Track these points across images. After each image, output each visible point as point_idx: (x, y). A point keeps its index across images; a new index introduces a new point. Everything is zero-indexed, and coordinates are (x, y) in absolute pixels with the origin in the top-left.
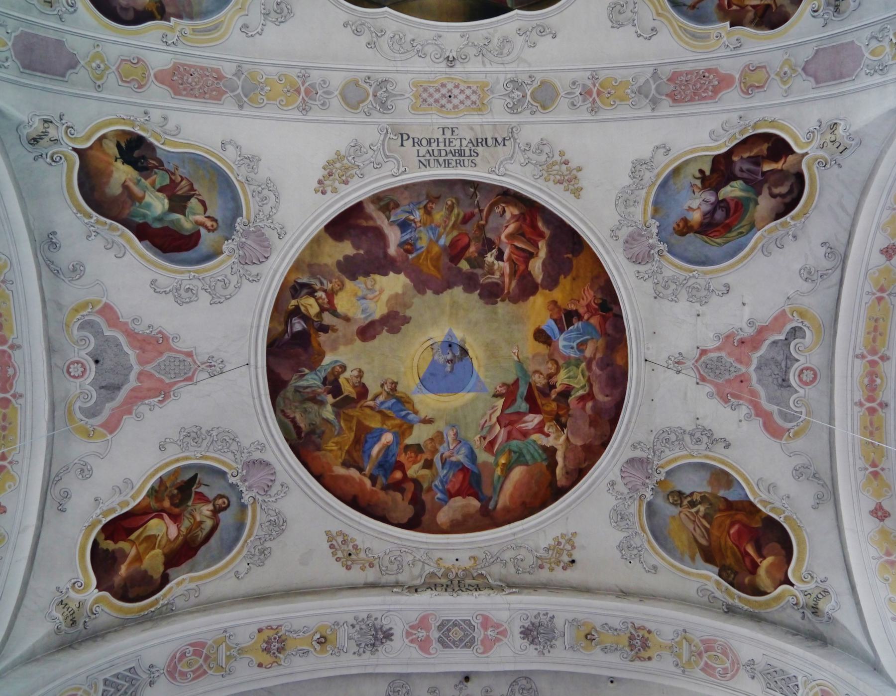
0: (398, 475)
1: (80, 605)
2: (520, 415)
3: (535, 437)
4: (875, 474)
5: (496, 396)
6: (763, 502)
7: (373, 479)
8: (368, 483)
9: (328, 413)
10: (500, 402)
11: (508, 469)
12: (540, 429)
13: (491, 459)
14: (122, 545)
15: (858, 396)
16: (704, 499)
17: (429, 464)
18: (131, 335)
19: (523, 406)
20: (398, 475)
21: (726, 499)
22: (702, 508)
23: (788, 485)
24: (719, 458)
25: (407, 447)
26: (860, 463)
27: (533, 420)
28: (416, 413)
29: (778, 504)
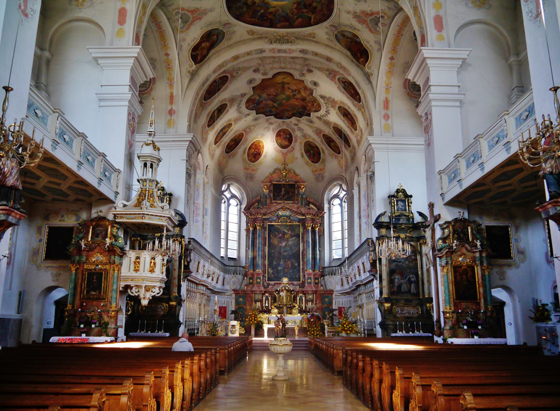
0: (266, 18)
1: (193, 71)
2: (302, 9)
3: (306, 14)
4: (394, 50)
5: (295, 3)
6: (365, 45)
7: (259, 19)
8: (257, 20)
9: (245, 9)
10: (296, 5)
11: (297, 19)
12: (307, 12)
13: (292, 16)
14: (197, 52)
15: (395, 33)
16: (350, 38)
17: (275, 16)
18: (188, 11)
19: (302, 6)
20: (266, 18)
21: (356, 40)
22: (349, 40)
23: (372, 43)
24: (355, 32)
25: (268, 13)
26: (391, 47)
27: (305, 10)
28: (270, 5)
29: (368, 46)
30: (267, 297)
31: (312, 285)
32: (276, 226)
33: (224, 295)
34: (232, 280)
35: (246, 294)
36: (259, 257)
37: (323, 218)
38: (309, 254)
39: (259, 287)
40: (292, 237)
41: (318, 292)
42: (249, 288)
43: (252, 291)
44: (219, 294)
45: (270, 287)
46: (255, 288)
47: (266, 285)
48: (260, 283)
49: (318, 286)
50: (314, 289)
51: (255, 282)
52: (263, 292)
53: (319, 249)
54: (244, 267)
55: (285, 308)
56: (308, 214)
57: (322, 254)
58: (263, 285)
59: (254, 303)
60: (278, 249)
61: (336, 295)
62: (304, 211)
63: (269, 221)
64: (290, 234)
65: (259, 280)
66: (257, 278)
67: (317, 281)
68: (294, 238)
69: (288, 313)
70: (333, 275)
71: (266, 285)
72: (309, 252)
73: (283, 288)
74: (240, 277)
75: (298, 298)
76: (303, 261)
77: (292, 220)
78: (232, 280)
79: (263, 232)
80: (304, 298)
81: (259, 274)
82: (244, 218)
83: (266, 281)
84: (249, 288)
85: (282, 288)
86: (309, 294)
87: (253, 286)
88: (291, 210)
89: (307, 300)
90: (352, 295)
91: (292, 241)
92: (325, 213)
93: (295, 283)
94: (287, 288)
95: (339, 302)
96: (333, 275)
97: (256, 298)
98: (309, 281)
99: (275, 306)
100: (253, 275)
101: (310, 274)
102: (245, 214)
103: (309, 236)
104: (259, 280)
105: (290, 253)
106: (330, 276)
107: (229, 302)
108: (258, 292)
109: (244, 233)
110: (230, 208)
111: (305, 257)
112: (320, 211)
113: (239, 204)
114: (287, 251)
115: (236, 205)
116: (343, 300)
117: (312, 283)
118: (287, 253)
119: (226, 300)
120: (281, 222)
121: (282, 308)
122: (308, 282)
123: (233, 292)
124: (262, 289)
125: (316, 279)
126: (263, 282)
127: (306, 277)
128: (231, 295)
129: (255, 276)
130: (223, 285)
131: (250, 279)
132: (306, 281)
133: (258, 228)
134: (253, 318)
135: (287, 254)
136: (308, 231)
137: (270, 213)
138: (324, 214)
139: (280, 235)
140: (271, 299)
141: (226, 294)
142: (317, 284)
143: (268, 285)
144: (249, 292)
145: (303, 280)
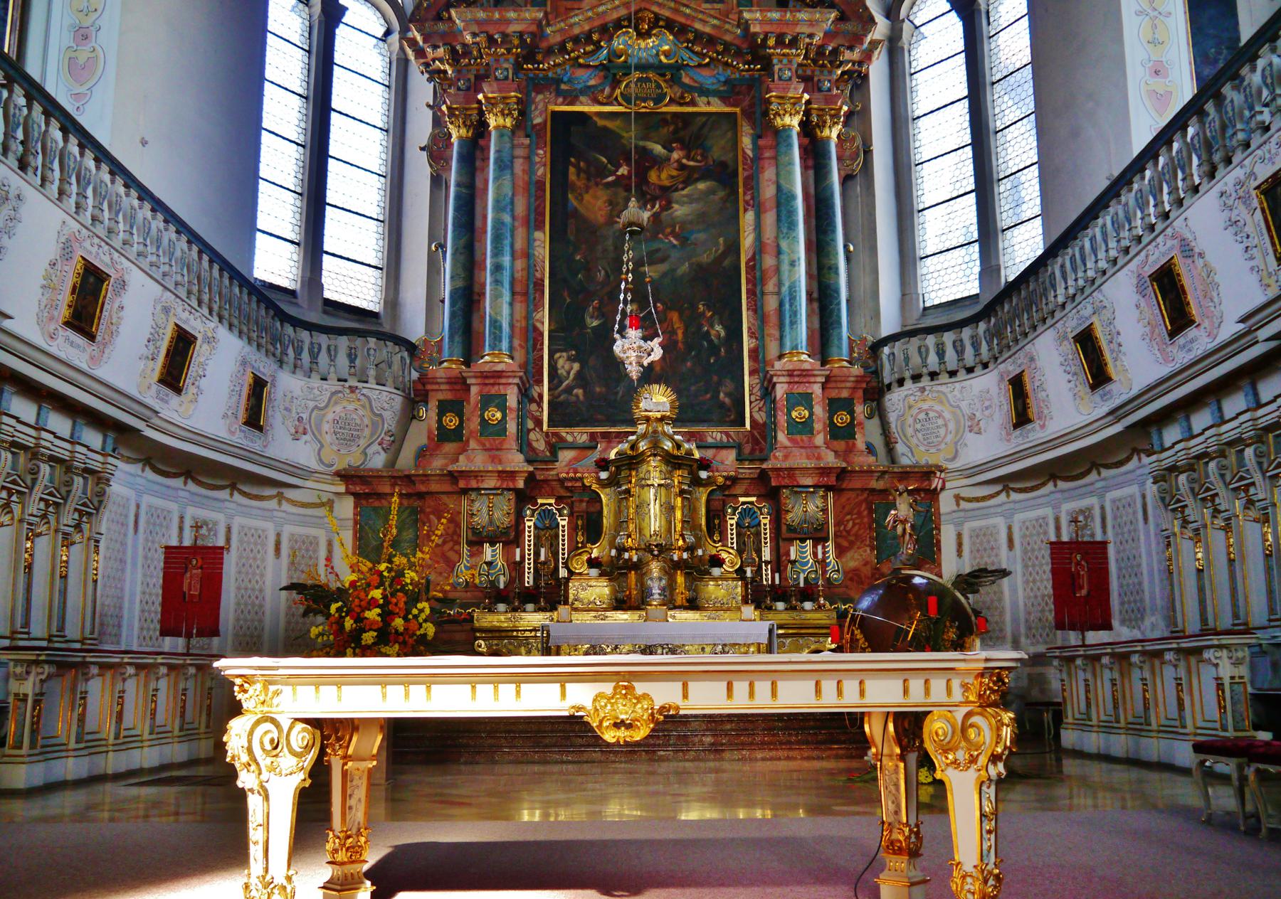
30: (547, 514)
31: (819, 440)
32: (601, 122)
33: (280, 497)
34: (330, 416)
35: (421, 496)
36: (497, 282)
37: (859, 81)
38: (793, 264)
39: (494, 452)
40: (687, 183)
41: (857, 483)
42: (437, 464)
43: (453, 477)
44: (233, 487)
45: (566, 456)
46: (475, 459)
47: (540, 445)
48: (501, 427)
49: (850, 450)
50: (830, 459)
51: (474, 424)
52: (520, 484)
53: (846, 247)
54: (411, 347)
55: (655, 568)
56: (780, 42)
57: (863, 282)
58: (524, 445)
59: (465, 549)
60: (609, 243)
61: (958, 498)
62: (762, 22)
63: (559, 93)
64: (682, 167)
65: (495, 415)
66: (486, 401)
67: (842, 419)
68: (701, 186)
69: (679, 600)
70: (944, 378)
71: (540, 445)
72: (793, 251)
73: (643, 446)
74: (388, 401)
75: (732, 522)
76: (756, 308)
77: (689, 89)
78: (330, 416)
79: (519, 152)
80: (765, 521)
81: (499, 375)
82: (422, 90)
83: (539, 423)
84: (437, 464)
85: (634, 446)
86: (797, 489)
87: (464, 450)
88: (679, 30)
89: (791, 529)
90: (1143, 465)
91: (691, 199)
92: (874, 44)
93: (715, 434)
94: (668, 445)
95: (983, 536)
96: (944, 378)
97: (481, 519)
98: (799, 413)
99: (593, 563)
100: (460, 384)
101: (805, 374)
102: (420, 53)
103: (791, 163)
104: (495, 415)
105: (685, 268)
106: (925, 381)
107: (314, 542)
108: (491, 483)
109: (419, 170)
110: (341, 32)
111: (770, 286)
112: (849, 27)
113: (396, 25)
114: (662, 260)
115: (380, 33)
116: (1019, 517)
117: (818, 426)
118: (663, 268)
119: (288, 530)
120: (627, 99)
121: (638, 567)
122: (792, 424)
123: (342, 489)
124: (516, 461)
125: (834, 405)
126: (523, 434)
127: (780, 391)
128: (330, 504)
129: (474, 390)
130: (254, 420)
131: (441, 414)
132: (782, 419)
133: (493, 121)
134: (373, 614)
135: (664, 275)
136: (780, 135)
137: (563, 49)
138: (867, 56)
139: (623, 171)
140: (573, 528)
141: (290, 493)
142: (842, 434)
143: (556, 446)
144: (434, 487)
145: (761, 417)
